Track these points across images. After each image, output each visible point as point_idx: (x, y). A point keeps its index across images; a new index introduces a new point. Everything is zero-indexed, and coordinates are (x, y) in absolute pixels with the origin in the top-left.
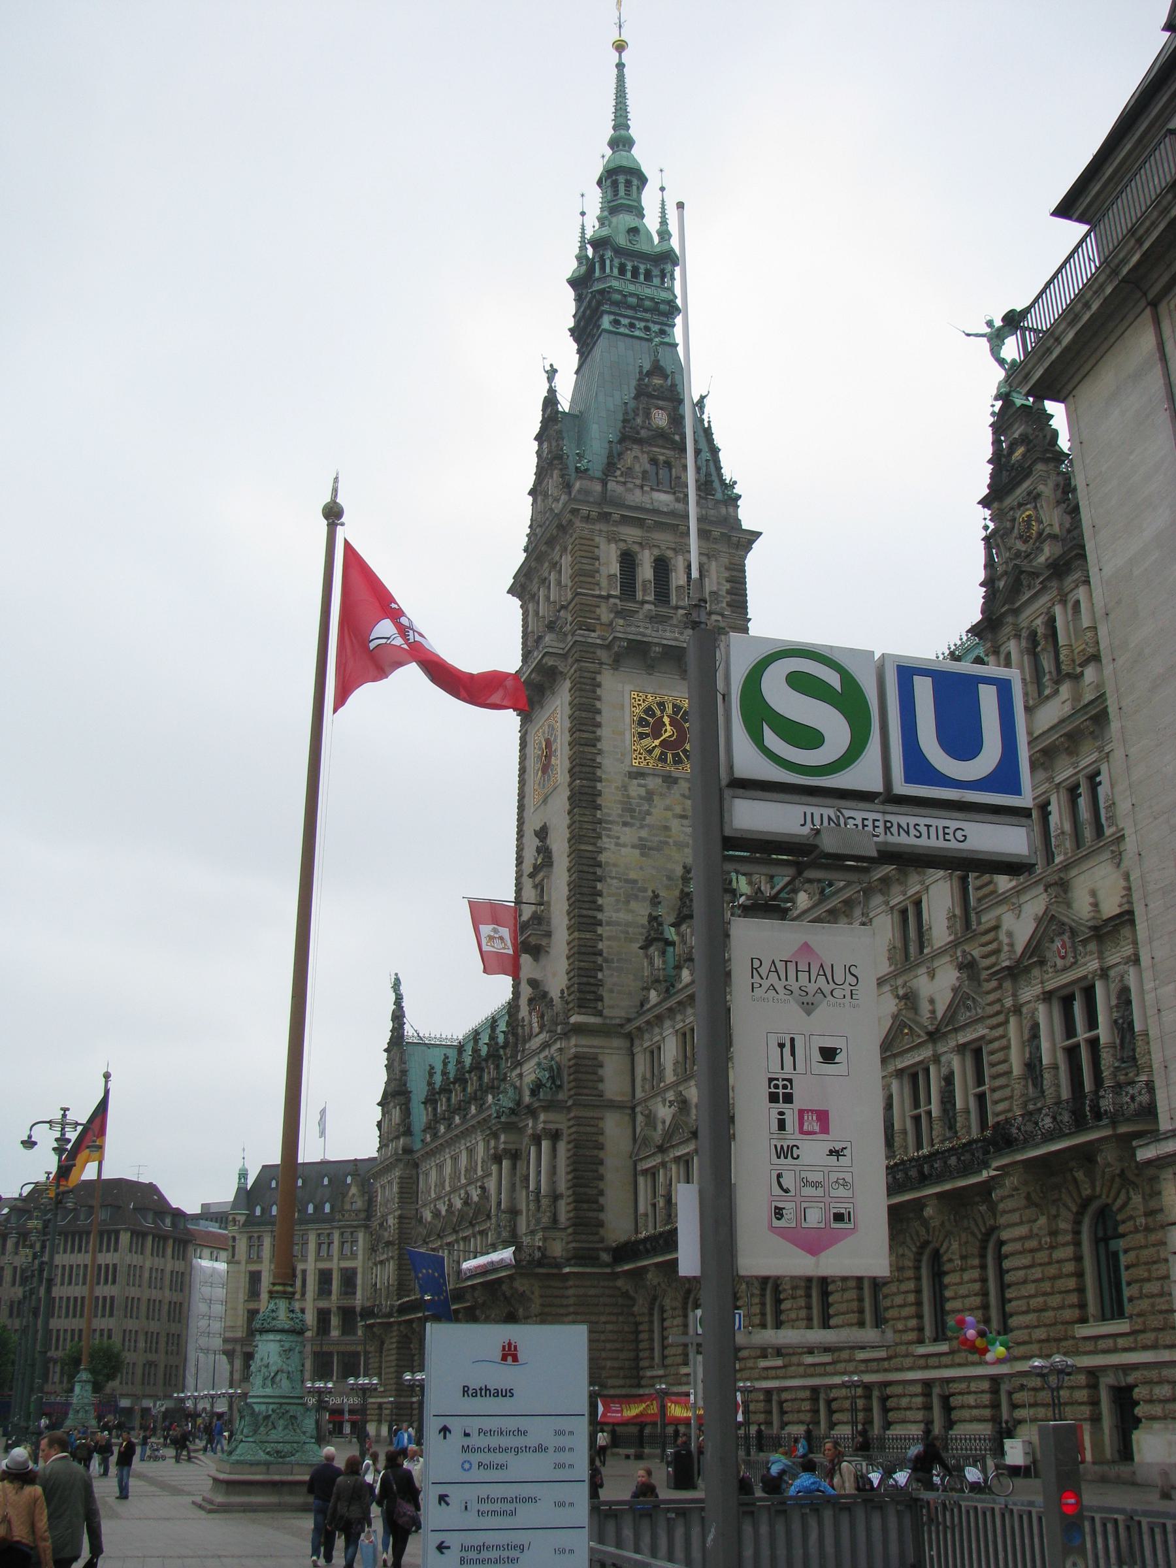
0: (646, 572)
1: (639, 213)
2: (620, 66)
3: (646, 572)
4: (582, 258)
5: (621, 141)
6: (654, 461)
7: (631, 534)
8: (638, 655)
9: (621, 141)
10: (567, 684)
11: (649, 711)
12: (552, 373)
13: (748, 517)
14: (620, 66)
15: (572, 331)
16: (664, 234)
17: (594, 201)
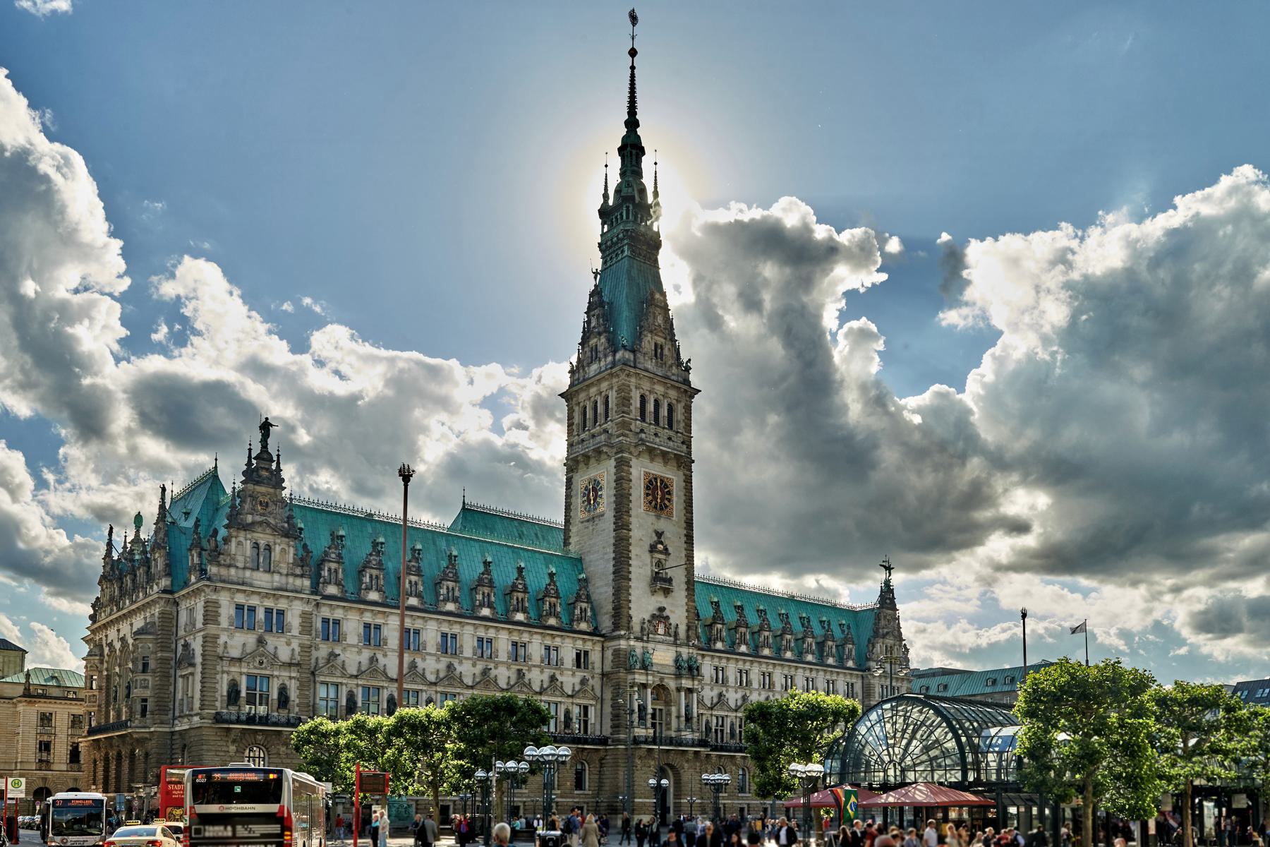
0: (650, 407)
1: (638, 173)
2: (633, 68)
3: (650, 407)
4: (606, 196)
5: (632, 123)
6: (656, 345)
7: (646, 385)
8: (651, 453)
9: (632, 123)
10: (612, 463)
11: (650, 482)
12: (596, 274)
13: (695, 380)
14: (633, 68)
15: (600, 245)
16: (656, 194)
17: (616, 162)
